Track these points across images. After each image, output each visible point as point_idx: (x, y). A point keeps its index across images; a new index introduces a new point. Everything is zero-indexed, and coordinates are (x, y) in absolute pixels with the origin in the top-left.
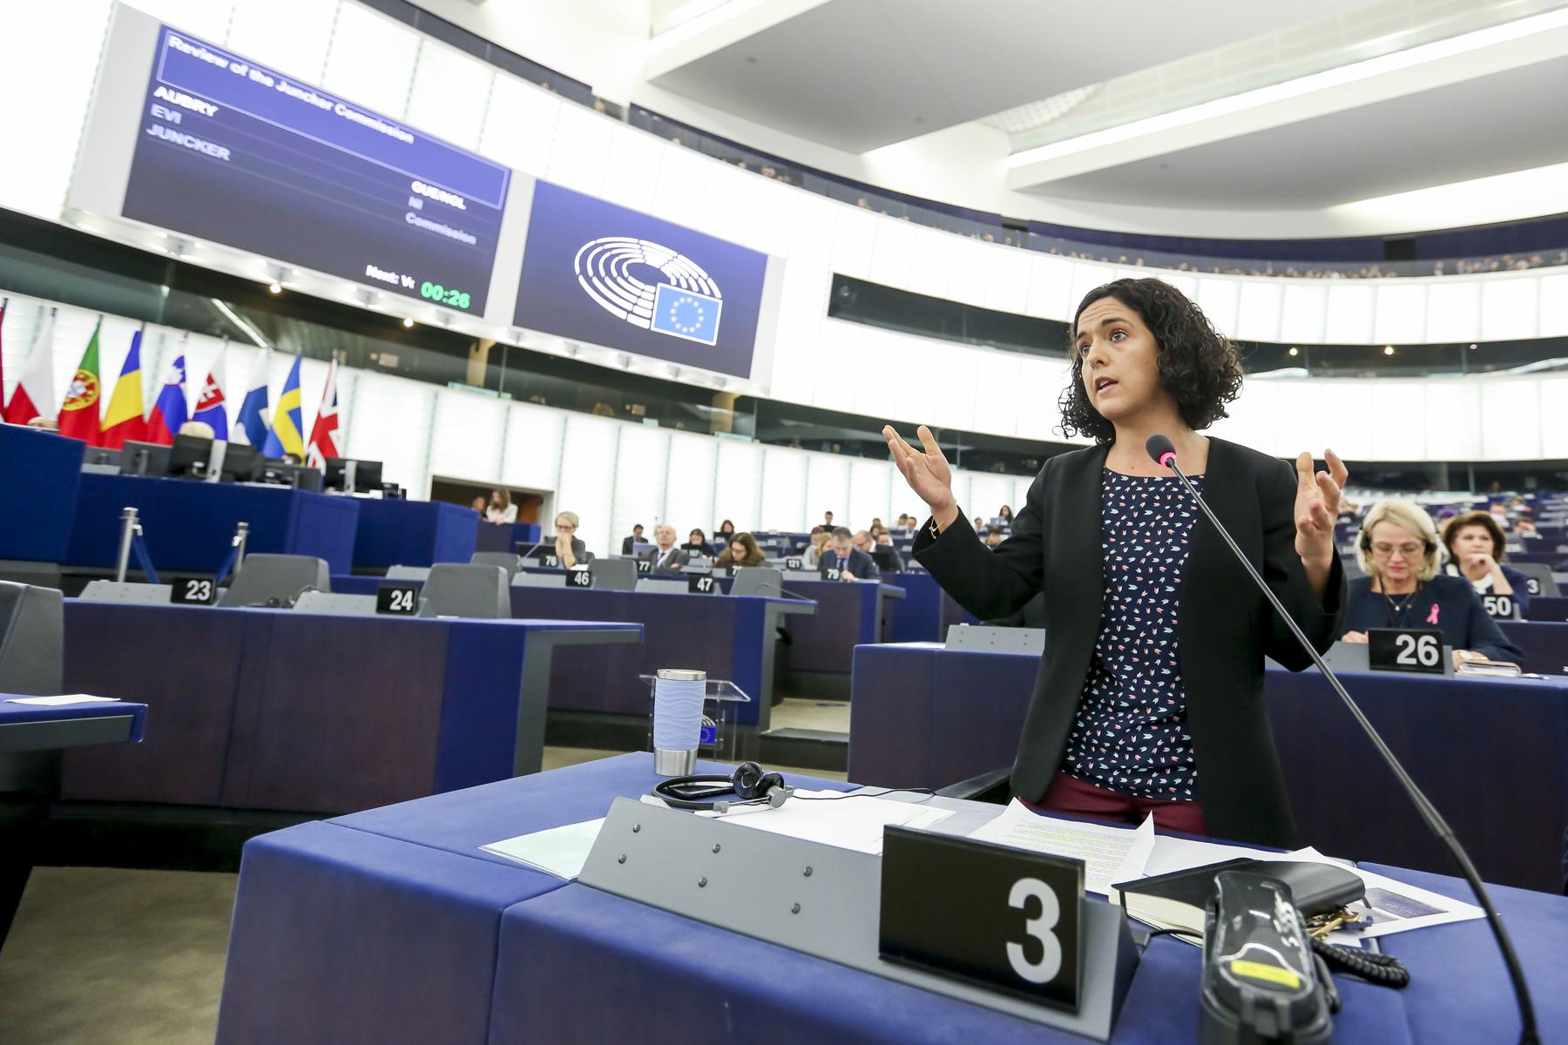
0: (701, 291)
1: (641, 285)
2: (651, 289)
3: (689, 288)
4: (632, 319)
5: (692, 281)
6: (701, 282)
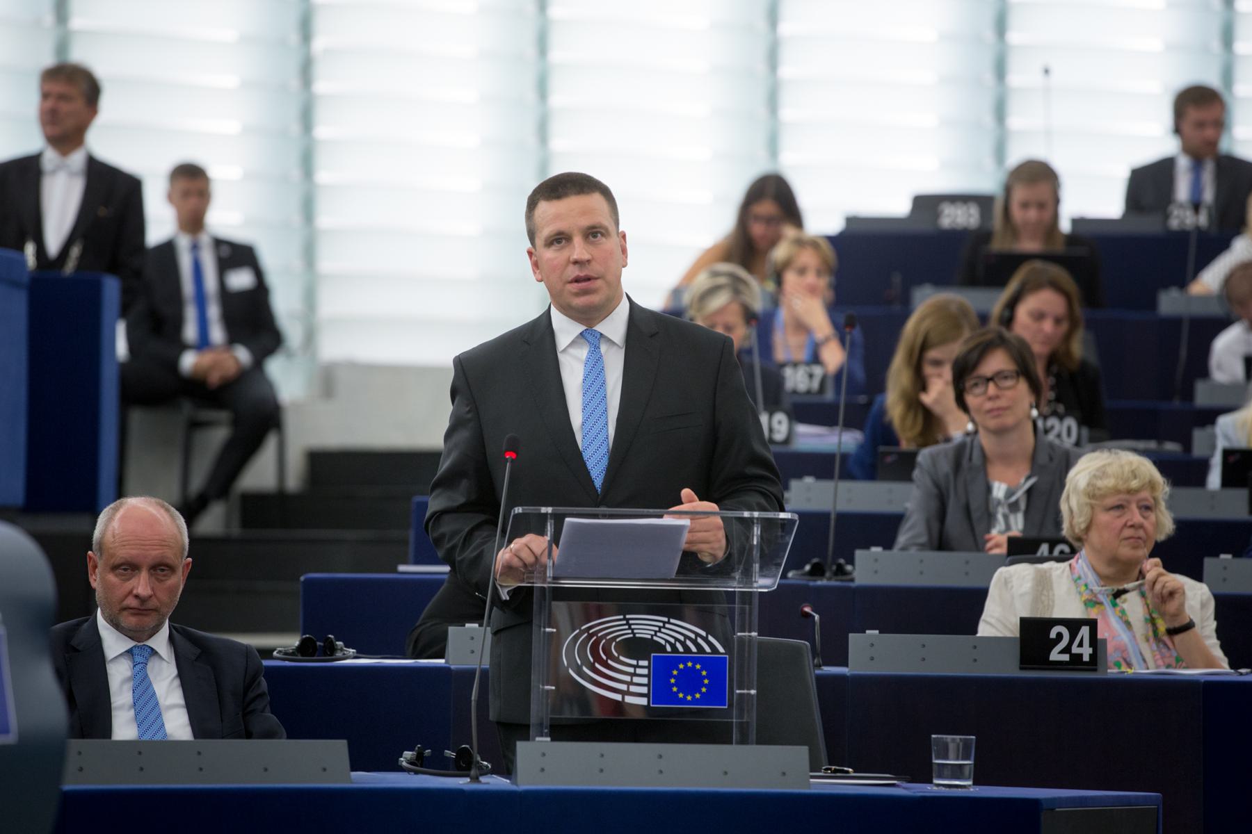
1: (634, 662)
2: (645, 663)
3: (687, 649)
4: (629, 699)
5: (688, 643)
6: (700, 640)
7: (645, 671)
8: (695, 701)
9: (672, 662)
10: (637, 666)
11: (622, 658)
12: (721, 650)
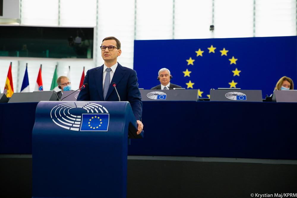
0: (100, 112)
1: (76, 117)
2: (80, 117)
3: (95, 112)
4: (72, 129)
5: (96, 109)
6: (100, 109)
7: (80, 120)
8: (96, 129)
9: (90, 116)
10: (77, 118)
11: (71, 115)
12: (107, 112)
